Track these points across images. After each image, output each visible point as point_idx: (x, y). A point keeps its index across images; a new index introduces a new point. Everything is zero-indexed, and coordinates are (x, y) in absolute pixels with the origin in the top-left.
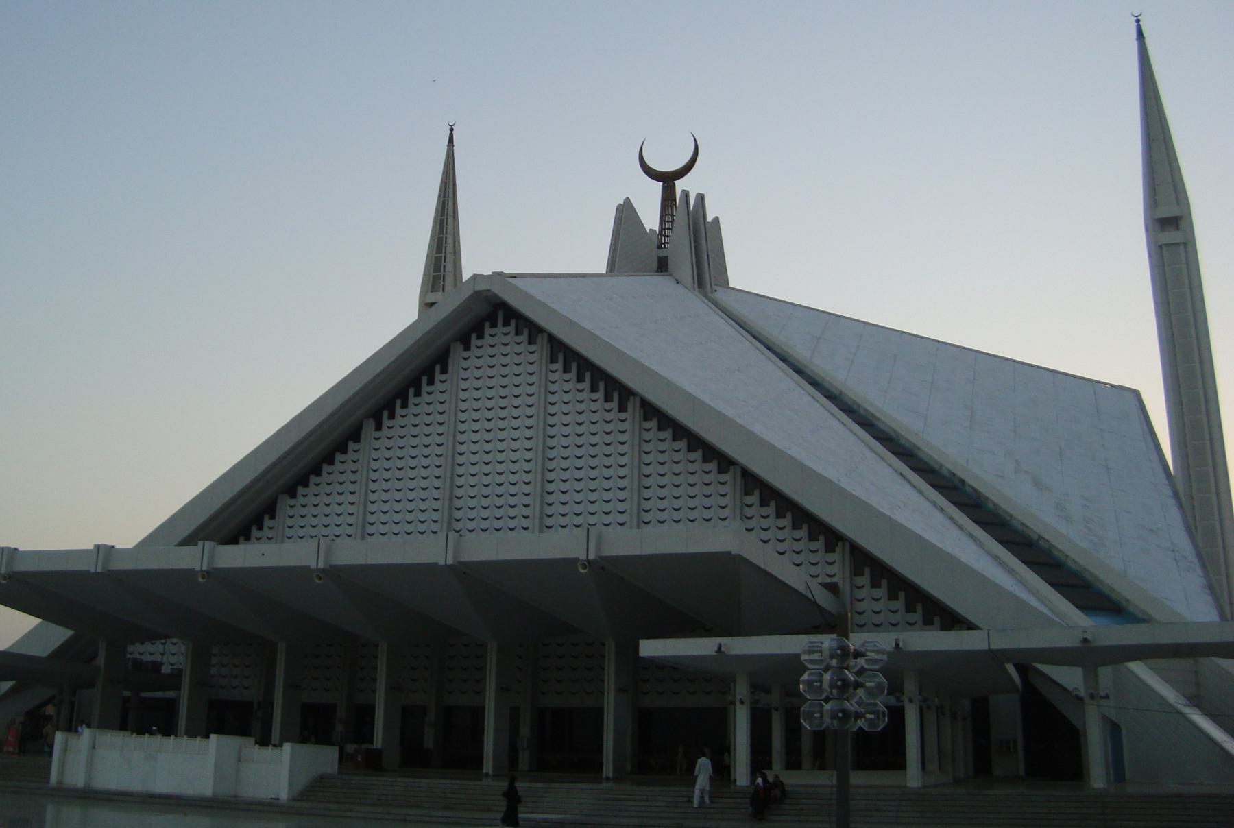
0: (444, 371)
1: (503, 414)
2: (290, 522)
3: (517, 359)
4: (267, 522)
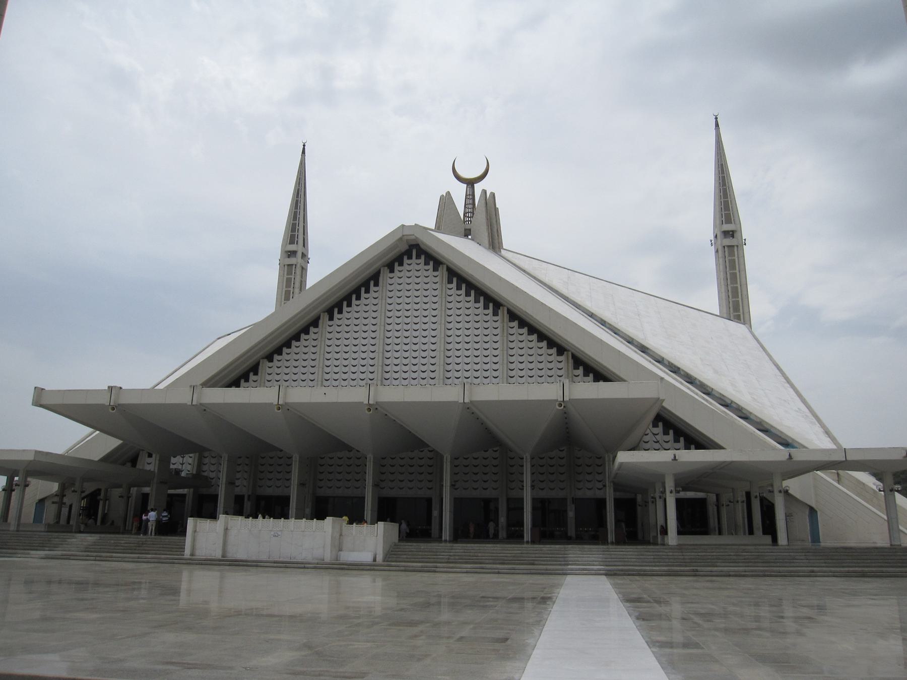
0: (376, 285)
3: (426, 280)
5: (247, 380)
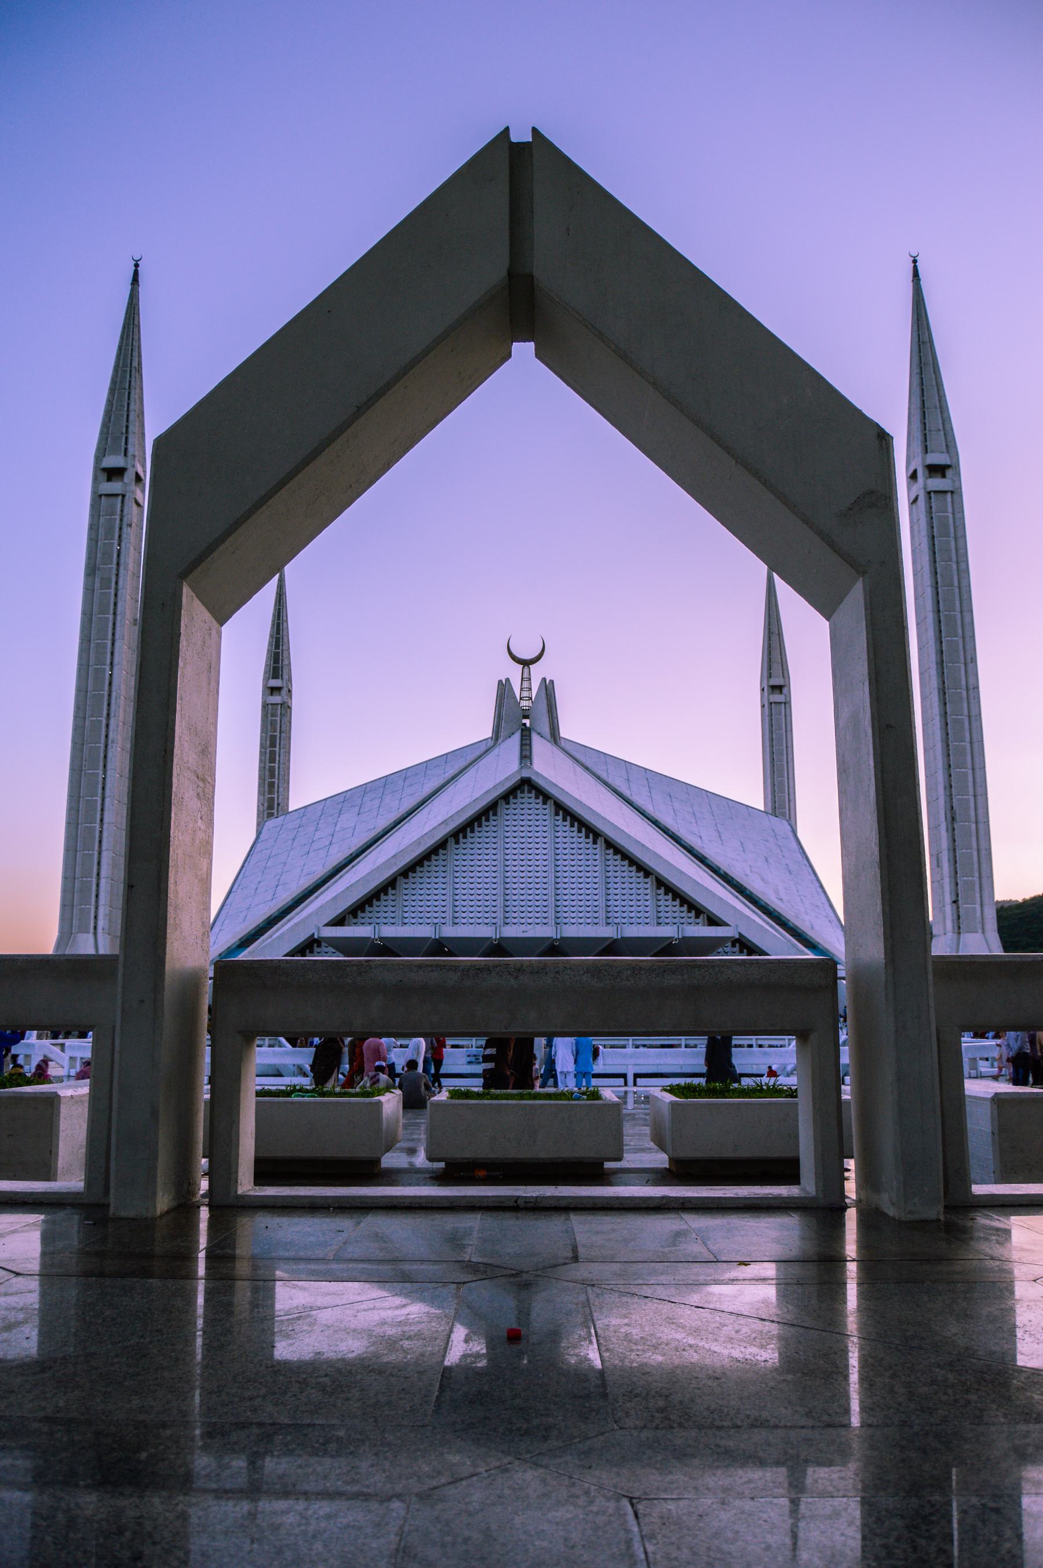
0: (495, 814)
1: (530, 840)
2: (406, 892)
3: (537, 812)
4: (390, 891)
5: (386, 894)
